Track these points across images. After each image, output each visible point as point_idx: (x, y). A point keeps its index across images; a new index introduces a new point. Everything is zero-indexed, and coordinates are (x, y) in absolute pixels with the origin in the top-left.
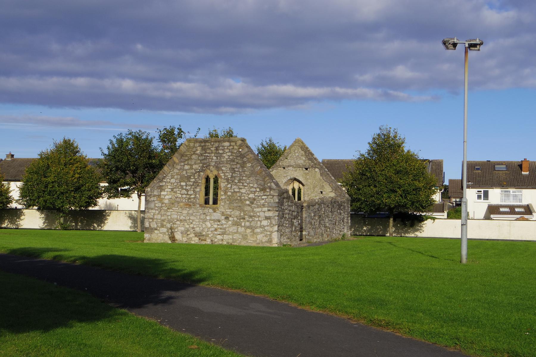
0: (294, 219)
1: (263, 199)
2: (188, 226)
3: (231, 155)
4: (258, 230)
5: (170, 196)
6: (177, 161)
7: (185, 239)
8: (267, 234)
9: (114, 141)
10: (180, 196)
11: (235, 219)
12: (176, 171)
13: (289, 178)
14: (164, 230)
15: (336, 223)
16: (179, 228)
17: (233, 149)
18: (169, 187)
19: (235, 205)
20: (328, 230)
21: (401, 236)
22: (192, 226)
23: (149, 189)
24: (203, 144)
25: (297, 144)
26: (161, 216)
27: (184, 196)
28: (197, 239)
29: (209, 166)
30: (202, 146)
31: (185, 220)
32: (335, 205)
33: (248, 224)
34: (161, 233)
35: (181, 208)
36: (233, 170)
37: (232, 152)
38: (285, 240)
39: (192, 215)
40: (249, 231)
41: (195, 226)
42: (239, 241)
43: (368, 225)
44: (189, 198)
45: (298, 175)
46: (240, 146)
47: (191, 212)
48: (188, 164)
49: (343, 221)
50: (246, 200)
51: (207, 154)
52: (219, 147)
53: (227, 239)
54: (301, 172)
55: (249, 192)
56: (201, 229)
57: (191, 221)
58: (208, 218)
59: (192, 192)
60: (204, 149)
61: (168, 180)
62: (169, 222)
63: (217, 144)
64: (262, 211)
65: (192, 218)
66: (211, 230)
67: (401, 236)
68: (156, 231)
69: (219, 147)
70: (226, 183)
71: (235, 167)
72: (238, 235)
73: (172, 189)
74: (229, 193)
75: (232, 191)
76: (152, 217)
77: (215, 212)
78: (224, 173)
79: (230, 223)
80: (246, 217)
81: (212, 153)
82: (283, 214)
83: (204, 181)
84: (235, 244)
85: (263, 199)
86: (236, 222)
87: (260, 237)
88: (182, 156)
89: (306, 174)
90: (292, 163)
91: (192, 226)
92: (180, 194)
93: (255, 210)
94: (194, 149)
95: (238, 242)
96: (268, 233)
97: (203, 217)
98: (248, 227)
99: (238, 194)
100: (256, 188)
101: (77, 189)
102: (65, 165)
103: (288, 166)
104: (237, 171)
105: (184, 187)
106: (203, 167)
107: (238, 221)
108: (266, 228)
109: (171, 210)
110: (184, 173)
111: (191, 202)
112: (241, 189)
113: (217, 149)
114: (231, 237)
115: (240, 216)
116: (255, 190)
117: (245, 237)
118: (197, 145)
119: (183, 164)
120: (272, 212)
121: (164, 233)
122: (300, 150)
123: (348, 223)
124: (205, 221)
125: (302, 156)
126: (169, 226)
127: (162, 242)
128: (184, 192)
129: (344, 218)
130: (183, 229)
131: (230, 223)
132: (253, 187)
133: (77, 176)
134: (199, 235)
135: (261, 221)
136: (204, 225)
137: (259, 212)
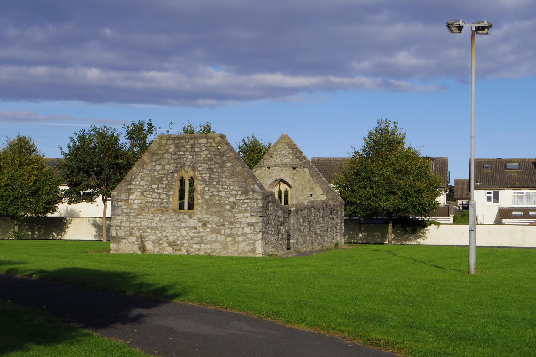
0: (281, 225)
1: (245, 203)
2: (160, 235)
3: (209, 154)
4: (240, 238)
5: (140, 201)
6: (147, 161)
7: (157, 249)
8: (250, 243)
9: (76, 138)
10: (151, 200)
11: (214, 226)
12: (146, 172)
13: (274, 179)
14: (133, 239)
15: (328, 229)
16: (151, 237)
17: (211, 146)
18: (138, 190)
19: (214, 210)
20: (319, 237)
21: (402, 244)
22: (164, 234)
23: (115, 193)
24: (176, 141)
25: (283, 141)
26: (130, 223)
27: (156, 200)
29: (184, 166)
30: (176, 144)
31: (157, 228)
32: (327, 209)
33: (228, 231)
34: (129, 243)
35: (152, 213)
37: (209, 150)
38: (270, 250)
39: (165, 221)
40: (229, 239)
41: (168, 235)
42: (218, 250)
43: (364, 231)
44: (162, 203)
45: (285, 175)
46: (219, 143)
47: (163, 218)
48: (160, 164)
49: (336, 228)
50: (226, 204)
51: (181, 153)
52: (195, 144)
53: (205, 249)
54: (289, 172)
55: (228, 195)
56: (175, 237)
57: (164, 229)
58: (183, 225)
59: (165, 196)
60: (178, 146)
61: (138, 182)
62: (139, 229)
63: (192, 142)
64: (244, 217)
66: (186, 238)
67: (402, 244)
68: (124, 241)
69: (195, 144)
72: (216, 244)
73: (142, 193)
74: (207, 197)
75: (210, 194)
76: (119, 224)
77: (190, 218)
78: (201, 174)
79: (208, 230)
80: (226, 223)
81: (187, 151)
82: (268, 220)
83: (178, 183)
84: (214, 254)
85: (245, 203)
86: (215, 229)
87: (242, 246)
88: (153, 154)
89: (294, 175)
90: (278, 162)
91: (164, 234)
92: (151, 198)
93: (236, 215)
94: (167, 147)
95: (217, 251)
96: (252, 242)
97: (176, 223)
98: (229, 235)
99: (217, 198)
100: (237, 191)
101: (34, 193)
102: (20, 166)
103: (274, 166)
104: (216, 172)
105: (156, 190)
107: (217, 228)
108: (249, 236)
109: (141, 217)
110: (156, 174)
111: (163, 207)
112: (220, 191)
113: (193, 146)
114: (209, 246)
115: (219, 222)
116: (236, 193)
117: (225, 246)
118: (170, 142)
119: (154, 164)
120: (255, 218)
121: (133, 243)
122: (287, 147)
123: (341, 229)
124: (179, 228)
125: (289, 154)
126: (138, 234)
127: (131, 252)
129: (337, 224)
130: (154, 237)
132: (233, 190)
133: (33, 178)
135: (243, 228)
136: (178, 233)
137: (241, 218)
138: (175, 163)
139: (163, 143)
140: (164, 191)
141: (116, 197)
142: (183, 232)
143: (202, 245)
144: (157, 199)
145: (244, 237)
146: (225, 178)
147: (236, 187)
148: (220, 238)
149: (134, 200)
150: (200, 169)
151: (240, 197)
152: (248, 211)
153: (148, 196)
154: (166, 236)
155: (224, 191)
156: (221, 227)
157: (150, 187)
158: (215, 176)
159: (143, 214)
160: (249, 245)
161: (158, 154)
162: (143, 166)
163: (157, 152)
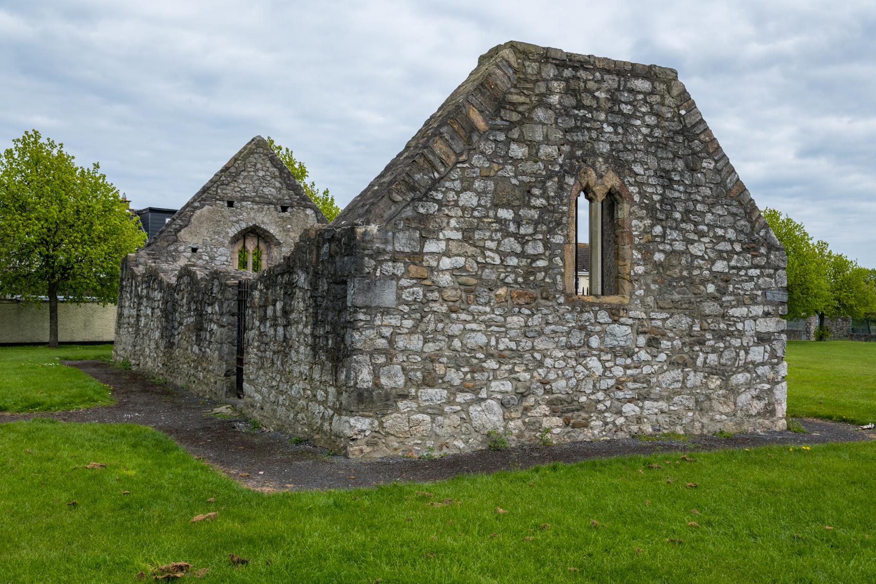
3: (657, 126)
4: (740, 378)
5: (461, 261)
8: (762, 391)
12: (477, 160)
13: (244, 226)
18: (453, 223)
19: (676, 297)
23: (374, 228)
24: (568, 73)
25: (261, 150)
26: (426, 341)
27: (513, 261)
28: (557, 421)
30: (567, 80)
31: (517, 354)
36: (665, 178)
37: (658, 115)
39: (541, 333)
40: (715, 382)
41: (552, 376)
44: (530, 271)
45: (265, 220)
47: (536, 320)
48: (520, 141)
50: (704, 282)
54: (275, 213)
59: (540, 249)
65: (540, 344)
66: (605, 384)
68: (401, 405)
70: (648, 222)
71: (668, 166)
74: (659, 257)
76: (382, 343)
77: (615, 321)
79: (662, 357)
85: (751, 278)
87: (743, 398)
92: (497, 251)
93: (731, 312)
94: (542, 88)
96: (767, 386)
97: (576, 338)
100: (732, 242)
103: (244, 199)
104: (678, 182)
106: (571, 156)
109: (463, 316)
111: (536, 286)
112: (692, 242)
113: (614, 99)
114: (663, 405)
116: (729, 248)
119: (502, 137)
122: (268, 164)
124: (582, 353)
125: (274, 178)
128: (510, 244)
130: (508, 386)
131: (662, 357)
132: (723, 238)
134: (557, 406)
136: (580, 368)
137: (743, 319)
138: (568, 142)
139: (529, 71)
140: (536, 232)
141: (378, 245)
142: (593, 363)
143: (646, 402)
144: (517, 255)
145: (748, 375)
146: (702, 202)
147: (730, 231)
148: (695, 379)
149: (440, 255)
150: (638, 169)
151: (738, 261)
152: (759, 299)
154: (544, 382)
155: (699, 241)
156: (697, 348)
157: (491, 213)
158: (677, 195)
159: (472, 307)
160: (758, 398)
161: (512, 104)
162: (469, 141)
163: (516, 98)
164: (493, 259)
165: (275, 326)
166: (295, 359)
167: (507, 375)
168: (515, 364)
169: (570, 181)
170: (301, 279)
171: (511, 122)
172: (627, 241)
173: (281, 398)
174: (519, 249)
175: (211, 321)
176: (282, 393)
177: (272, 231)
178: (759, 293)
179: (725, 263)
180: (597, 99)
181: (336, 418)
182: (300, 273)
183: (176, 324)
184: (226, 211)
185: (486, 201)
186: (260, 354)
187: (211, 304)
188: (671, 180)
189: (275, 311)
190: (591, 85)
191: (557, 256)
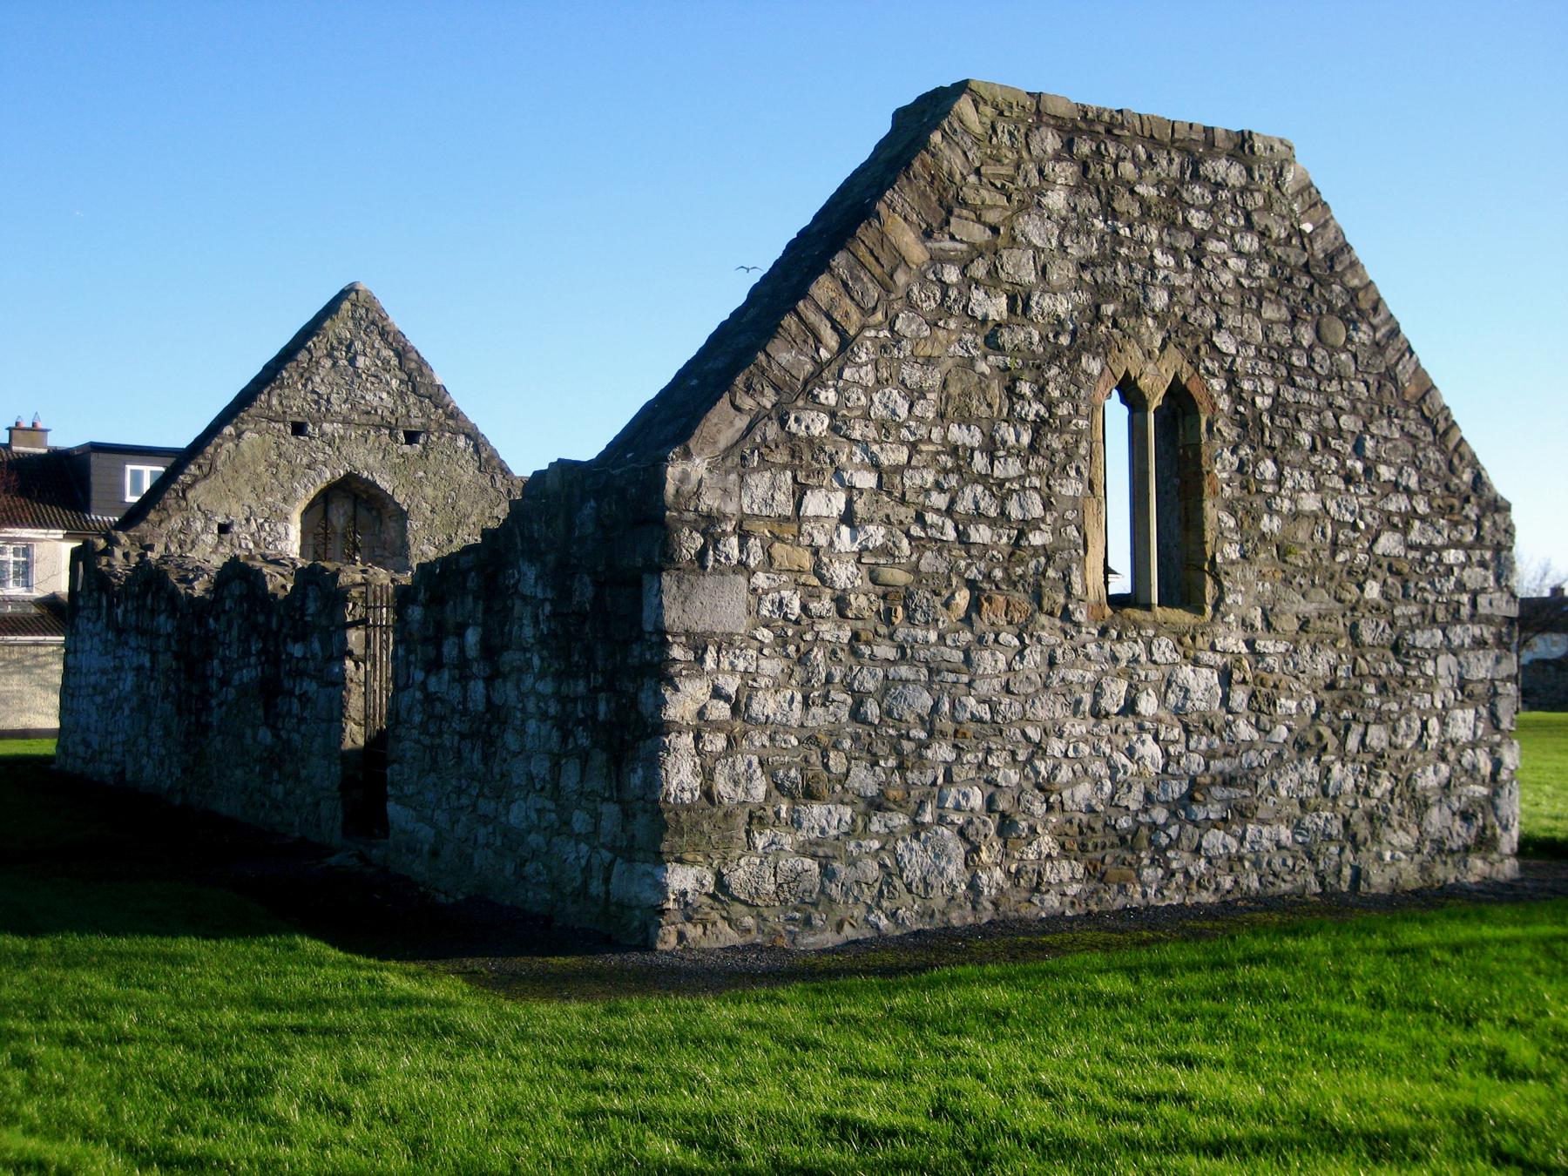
23: (698, 467)
27: (981, 534)
37: (1263, 234)
71: (1284, 338)
92: (949, 512)
105: (980, 462)
131: (1281, 733)
144: (992, 523)
150: (1225, 342)
153: (940, 500)
157: (936, 434)
164: (942, 530)
165: (463, 679)
166: (514, 747)
167: (972, 774)
168: (989, 751)
169: (1094, 366)
170: (528, 577)
171: (972, 245)
172: (1207, 490)
173: (482, 832)
174: (993, 513)
175: (300, 674)
176: (485, 820)
177: (383, 484)
178: (1465, 598)
179: (1398, 536)
180: (1142, 200)
181: (619, 866)
182: (525, 567)
183: (214, 685)
184: (291, 443)
185: (927, 409)
186: (427, 741)
187: (302, 637)
188: (1290, 367)
189: (462, 650)
190: (1127, 169)
191: (1070, 523)
